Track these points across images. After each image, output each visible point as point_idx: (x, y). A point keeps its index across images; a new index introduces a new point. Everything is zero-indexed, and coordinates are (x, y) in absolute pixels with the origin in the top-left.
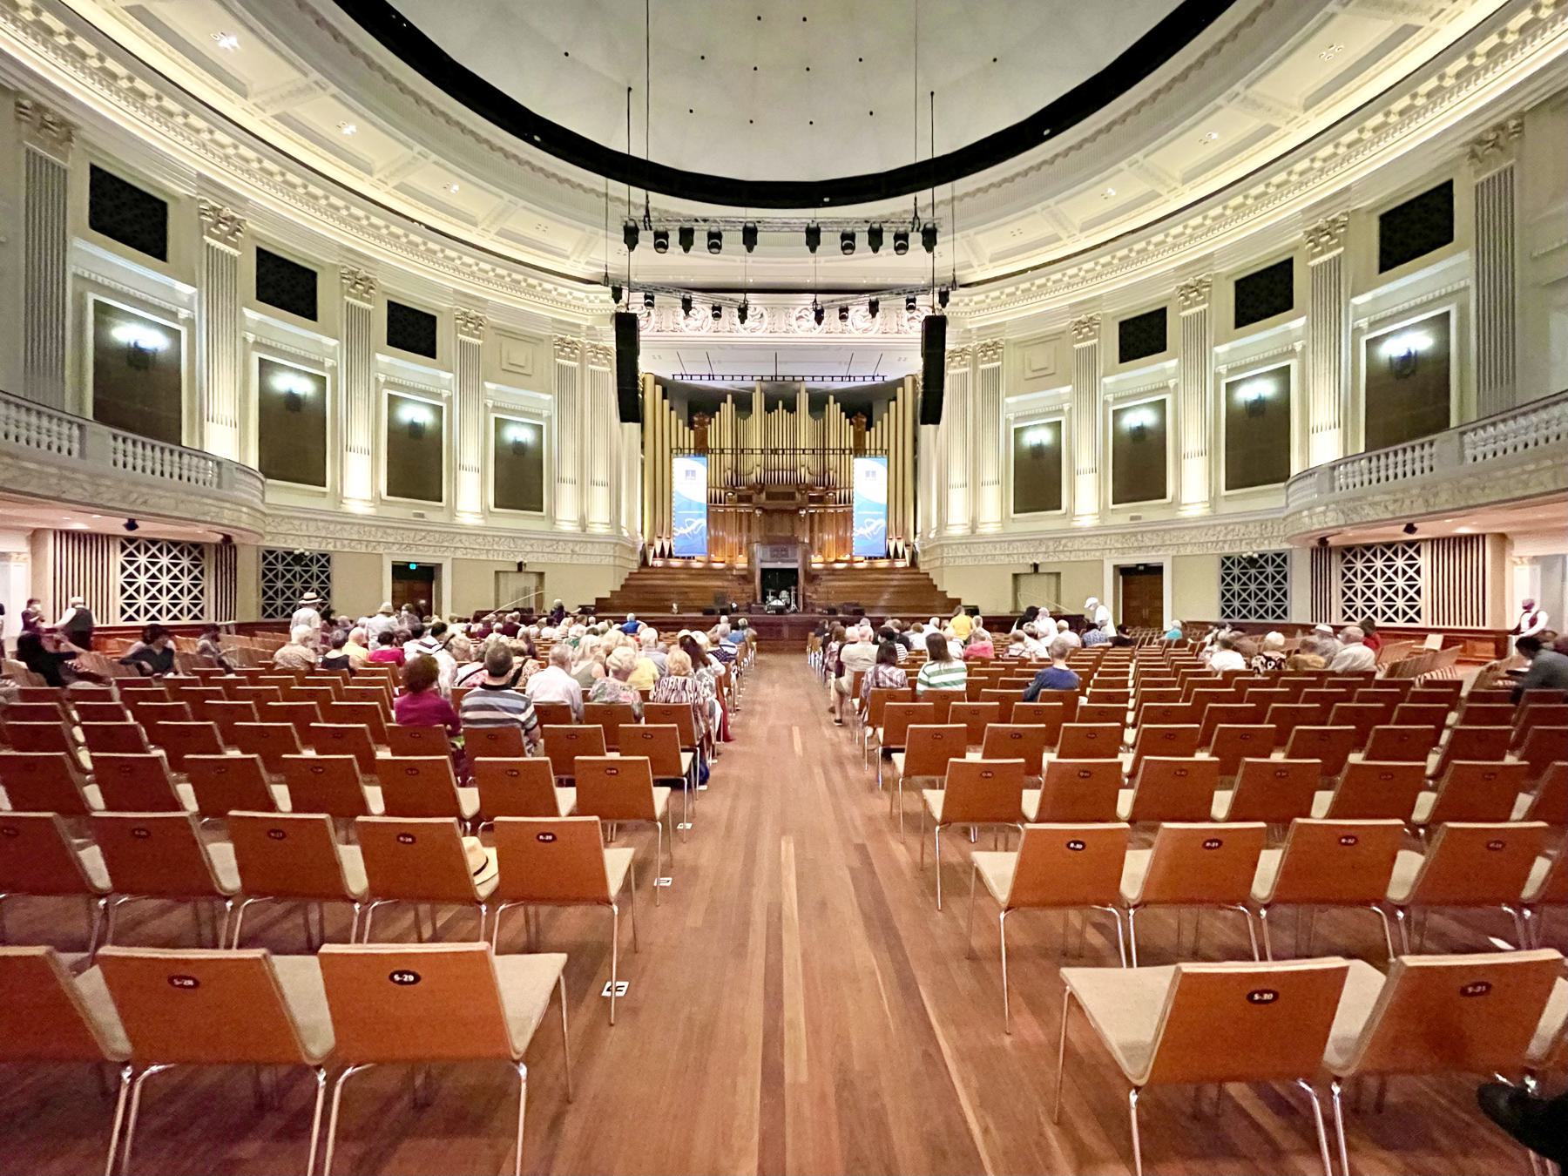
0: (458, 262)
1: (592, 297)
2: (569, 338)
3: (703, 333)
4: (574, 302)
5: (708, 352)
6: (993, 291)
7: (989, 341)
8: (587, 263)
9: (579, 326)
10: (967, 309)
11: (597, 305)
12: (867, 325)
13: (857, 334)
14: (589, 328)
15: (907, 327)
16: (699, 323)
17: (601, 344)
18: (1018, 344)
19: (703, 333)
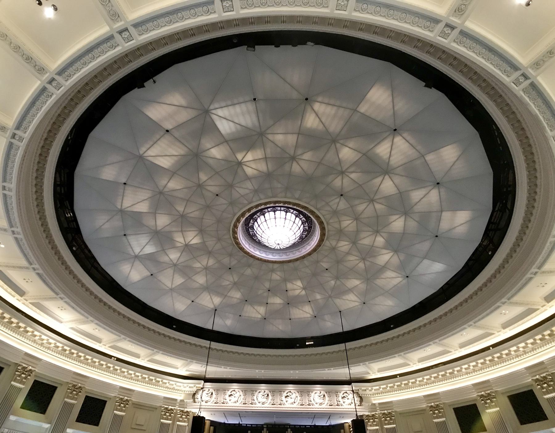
0: (126, 373)
1: (185, 385)
2: (170, 407)
3: (237, 404)
4: (176, 388)
5: (239, 414)
6: (382, 385)
7: (386, 411)
8: (186, 370)
9: (176, 400)
10: (371, 393)
11: (188, 389)
12: (321, 401)
13: (317, 406)
14: (182, 401)
15: (342, 402)
16: (236, 399)
17: (186, 410)
18: (401, 414)
19: (237, 404)
